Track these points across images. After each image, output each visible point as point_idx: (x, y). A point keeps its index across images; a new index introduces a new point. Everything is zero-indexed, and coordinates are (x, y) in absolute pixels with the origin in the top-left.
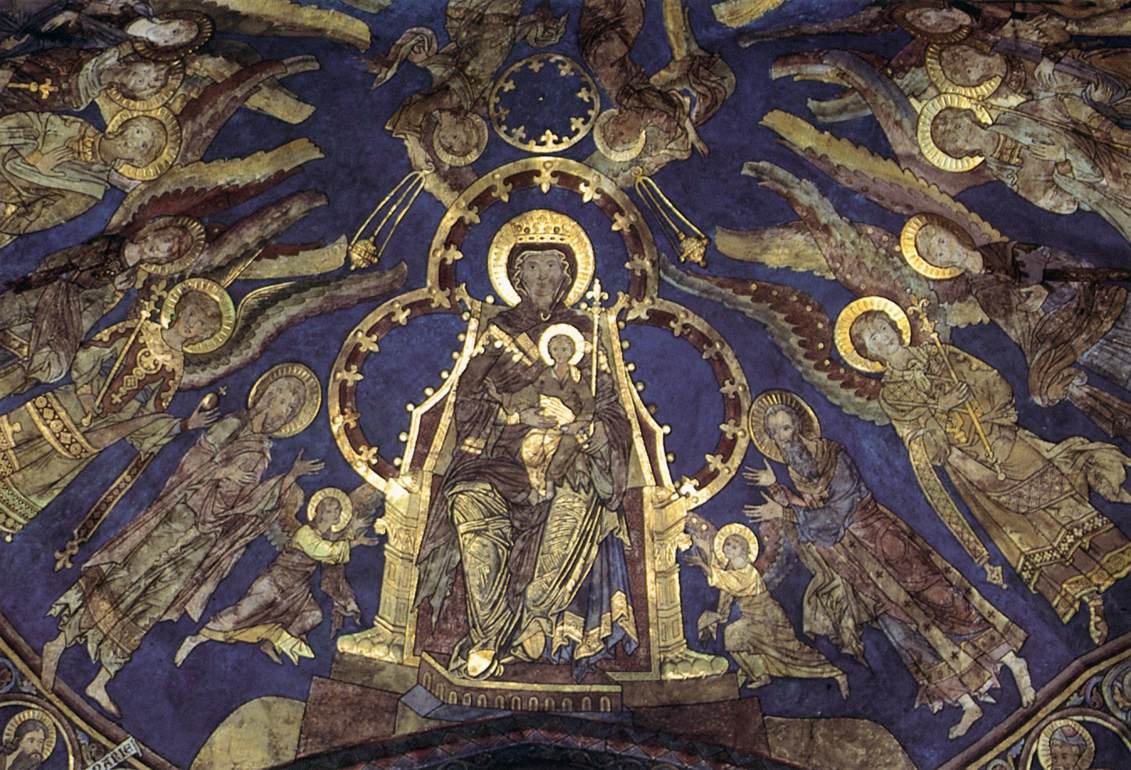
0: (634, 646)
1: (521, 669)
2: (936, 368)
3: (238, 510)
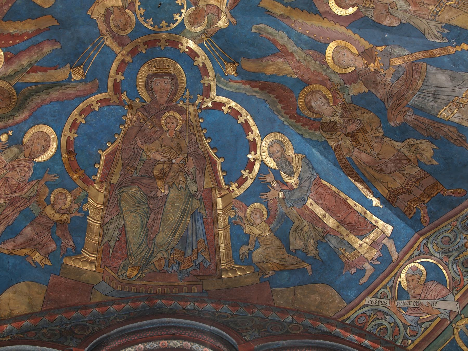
0: (209, 264)
2: (345, 114)
3: (17, 194)
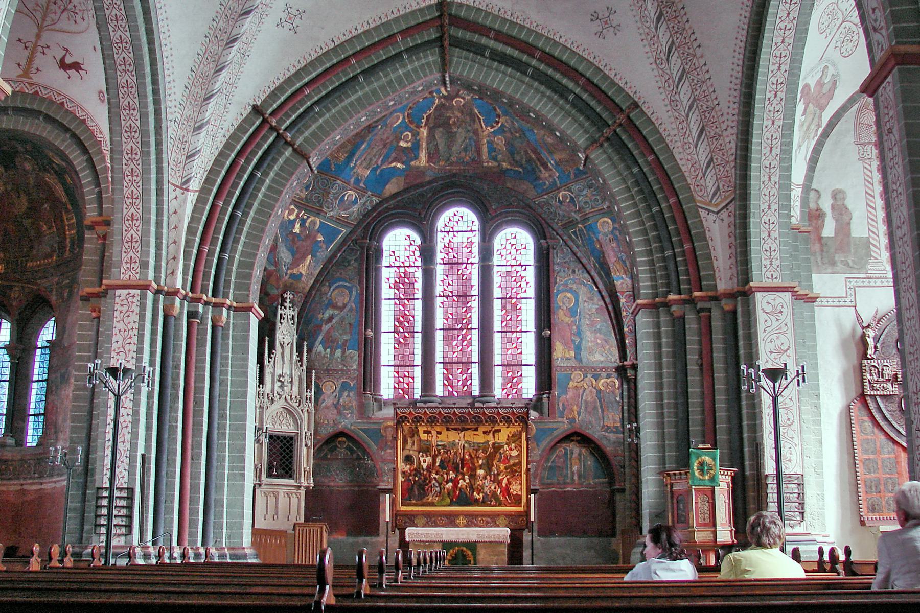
1: (451, 164)
